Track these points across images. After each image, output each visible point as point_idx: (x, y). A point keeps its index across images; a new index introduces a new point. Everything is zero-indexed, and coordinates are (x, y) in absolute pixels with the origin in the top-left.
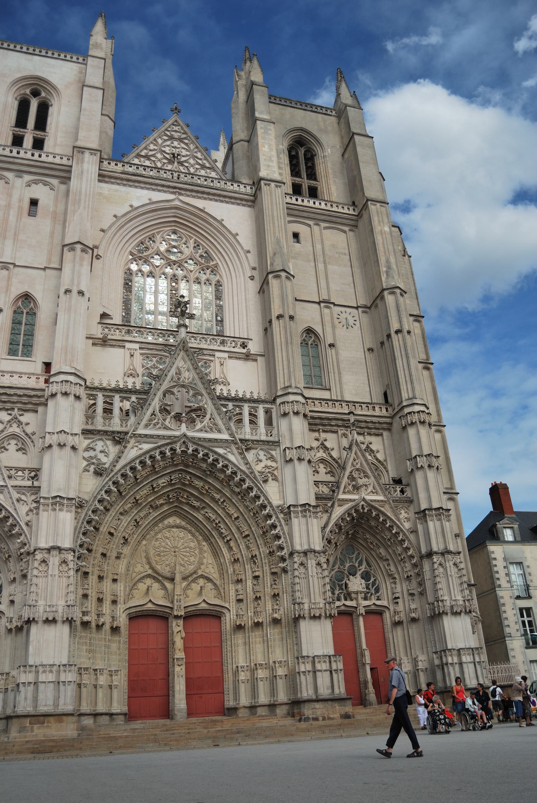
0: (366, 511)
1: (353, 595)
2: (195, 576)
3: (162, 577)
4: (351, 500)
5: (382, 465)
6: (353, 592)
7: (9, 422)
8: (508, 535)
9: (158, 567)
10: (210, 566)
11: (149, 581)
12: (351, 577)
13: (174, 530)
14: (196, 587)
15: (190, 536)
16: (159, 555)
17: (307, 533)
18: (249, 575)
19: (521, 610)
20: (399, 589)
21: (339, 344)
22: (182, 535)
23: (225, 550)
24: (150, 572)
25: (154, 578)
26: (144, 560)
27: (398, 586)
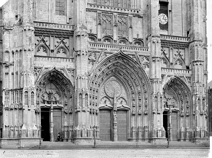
1: (169, 106)
2: (119, 97)
3: (109, 97)
5: (183, 60)
7: (60, 42)
9: (108, 94)
11: (105, 98)
14: (120, 101)
15: (118, 84)
17: (159, 88)
18: (137, 98)
21: (173, 11)
23: (130, 89)
24: (105, 95)
26: (104, 91)
27: (184, 104)
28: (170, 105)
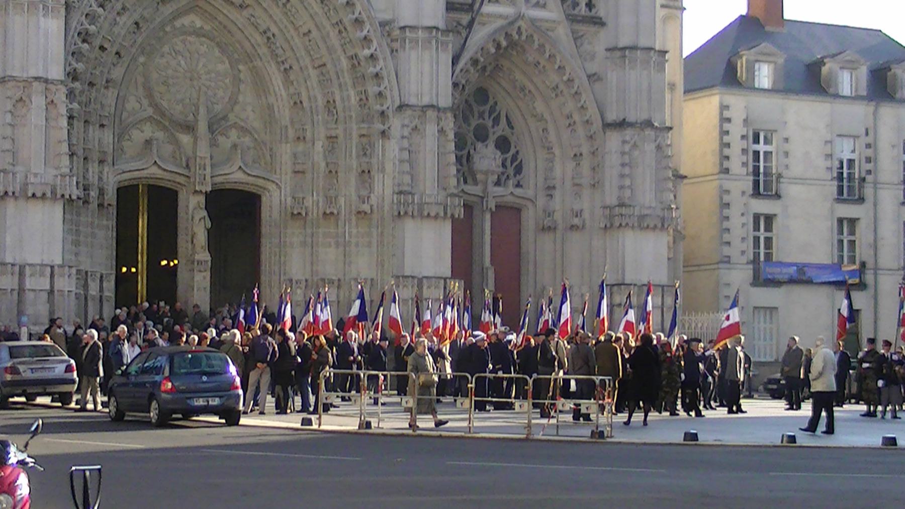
0: (524, 37)
1: (479, 177)
4: (501, 16)
6: (481, 172)
8: (764, 76)
9: (165, 104)
10: (249, 108)
12: (479, 145)
13: (191, 39)
15: (217, 52)
16: (164, 83)
18: (322, 133)
19: (757, 217)
20: (558, 172)
22: (203, 49)
24: (150, 111)
25: (158, 123)
26: (141, 89)
28: (486, 173)
